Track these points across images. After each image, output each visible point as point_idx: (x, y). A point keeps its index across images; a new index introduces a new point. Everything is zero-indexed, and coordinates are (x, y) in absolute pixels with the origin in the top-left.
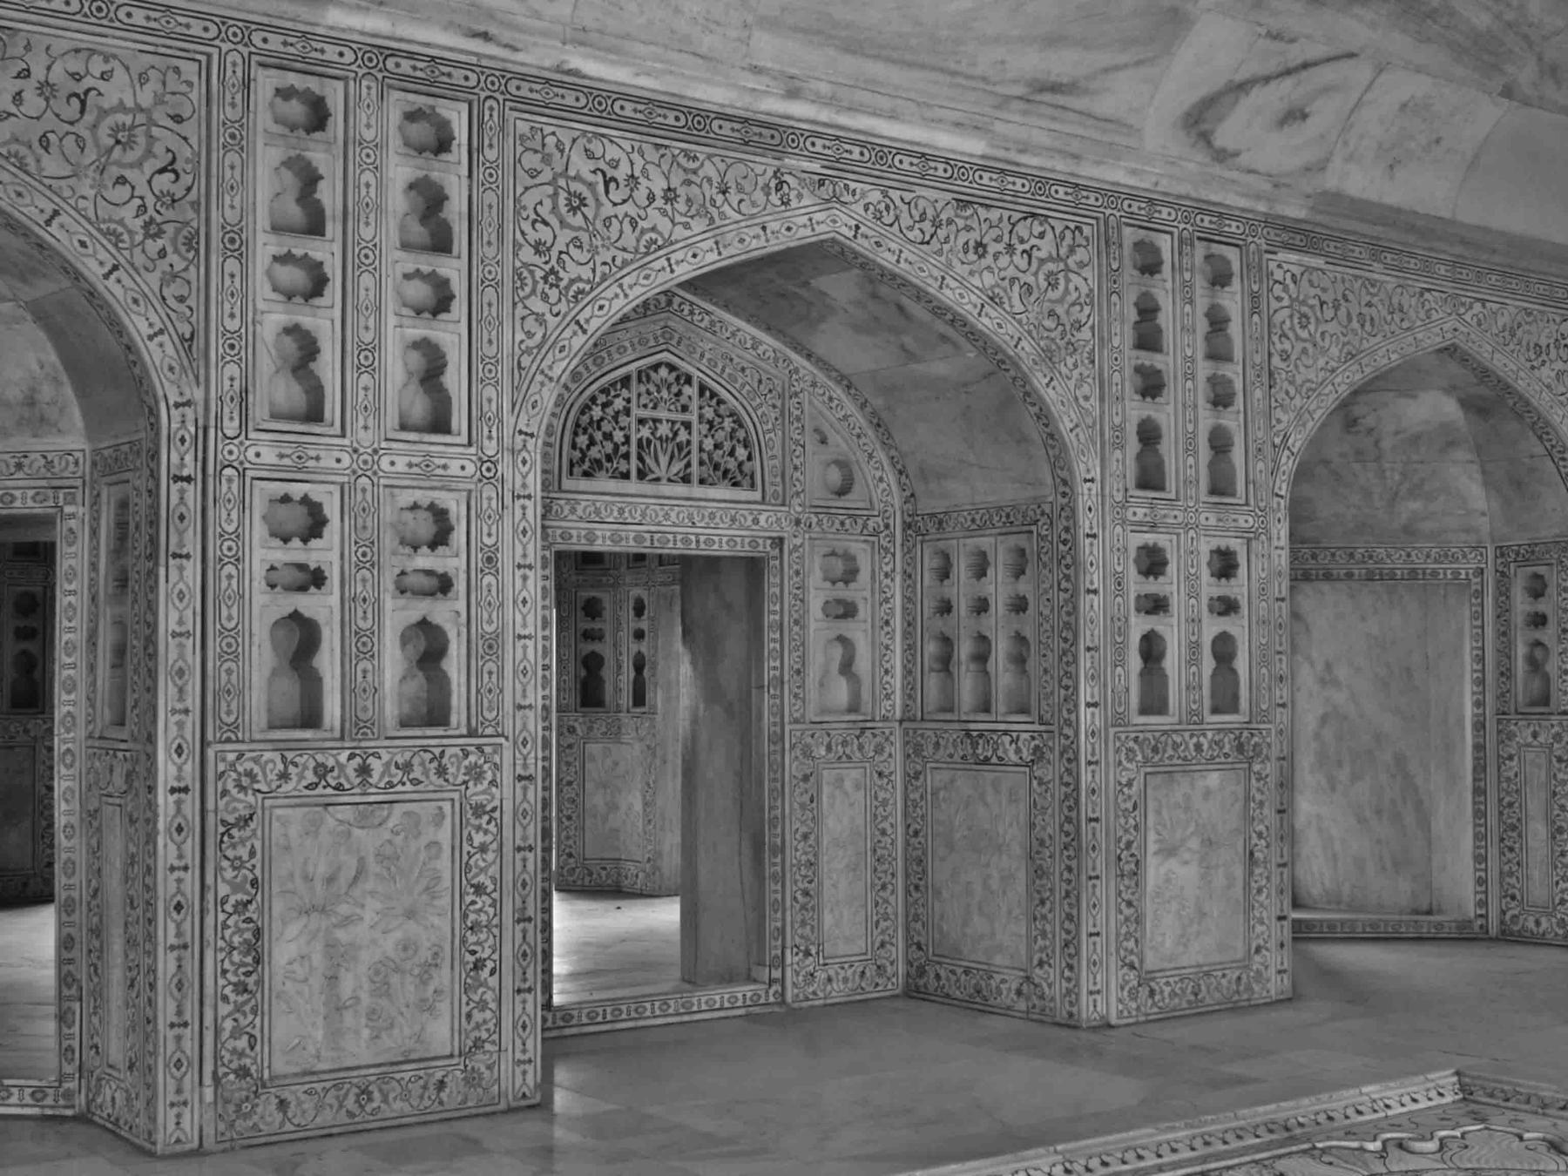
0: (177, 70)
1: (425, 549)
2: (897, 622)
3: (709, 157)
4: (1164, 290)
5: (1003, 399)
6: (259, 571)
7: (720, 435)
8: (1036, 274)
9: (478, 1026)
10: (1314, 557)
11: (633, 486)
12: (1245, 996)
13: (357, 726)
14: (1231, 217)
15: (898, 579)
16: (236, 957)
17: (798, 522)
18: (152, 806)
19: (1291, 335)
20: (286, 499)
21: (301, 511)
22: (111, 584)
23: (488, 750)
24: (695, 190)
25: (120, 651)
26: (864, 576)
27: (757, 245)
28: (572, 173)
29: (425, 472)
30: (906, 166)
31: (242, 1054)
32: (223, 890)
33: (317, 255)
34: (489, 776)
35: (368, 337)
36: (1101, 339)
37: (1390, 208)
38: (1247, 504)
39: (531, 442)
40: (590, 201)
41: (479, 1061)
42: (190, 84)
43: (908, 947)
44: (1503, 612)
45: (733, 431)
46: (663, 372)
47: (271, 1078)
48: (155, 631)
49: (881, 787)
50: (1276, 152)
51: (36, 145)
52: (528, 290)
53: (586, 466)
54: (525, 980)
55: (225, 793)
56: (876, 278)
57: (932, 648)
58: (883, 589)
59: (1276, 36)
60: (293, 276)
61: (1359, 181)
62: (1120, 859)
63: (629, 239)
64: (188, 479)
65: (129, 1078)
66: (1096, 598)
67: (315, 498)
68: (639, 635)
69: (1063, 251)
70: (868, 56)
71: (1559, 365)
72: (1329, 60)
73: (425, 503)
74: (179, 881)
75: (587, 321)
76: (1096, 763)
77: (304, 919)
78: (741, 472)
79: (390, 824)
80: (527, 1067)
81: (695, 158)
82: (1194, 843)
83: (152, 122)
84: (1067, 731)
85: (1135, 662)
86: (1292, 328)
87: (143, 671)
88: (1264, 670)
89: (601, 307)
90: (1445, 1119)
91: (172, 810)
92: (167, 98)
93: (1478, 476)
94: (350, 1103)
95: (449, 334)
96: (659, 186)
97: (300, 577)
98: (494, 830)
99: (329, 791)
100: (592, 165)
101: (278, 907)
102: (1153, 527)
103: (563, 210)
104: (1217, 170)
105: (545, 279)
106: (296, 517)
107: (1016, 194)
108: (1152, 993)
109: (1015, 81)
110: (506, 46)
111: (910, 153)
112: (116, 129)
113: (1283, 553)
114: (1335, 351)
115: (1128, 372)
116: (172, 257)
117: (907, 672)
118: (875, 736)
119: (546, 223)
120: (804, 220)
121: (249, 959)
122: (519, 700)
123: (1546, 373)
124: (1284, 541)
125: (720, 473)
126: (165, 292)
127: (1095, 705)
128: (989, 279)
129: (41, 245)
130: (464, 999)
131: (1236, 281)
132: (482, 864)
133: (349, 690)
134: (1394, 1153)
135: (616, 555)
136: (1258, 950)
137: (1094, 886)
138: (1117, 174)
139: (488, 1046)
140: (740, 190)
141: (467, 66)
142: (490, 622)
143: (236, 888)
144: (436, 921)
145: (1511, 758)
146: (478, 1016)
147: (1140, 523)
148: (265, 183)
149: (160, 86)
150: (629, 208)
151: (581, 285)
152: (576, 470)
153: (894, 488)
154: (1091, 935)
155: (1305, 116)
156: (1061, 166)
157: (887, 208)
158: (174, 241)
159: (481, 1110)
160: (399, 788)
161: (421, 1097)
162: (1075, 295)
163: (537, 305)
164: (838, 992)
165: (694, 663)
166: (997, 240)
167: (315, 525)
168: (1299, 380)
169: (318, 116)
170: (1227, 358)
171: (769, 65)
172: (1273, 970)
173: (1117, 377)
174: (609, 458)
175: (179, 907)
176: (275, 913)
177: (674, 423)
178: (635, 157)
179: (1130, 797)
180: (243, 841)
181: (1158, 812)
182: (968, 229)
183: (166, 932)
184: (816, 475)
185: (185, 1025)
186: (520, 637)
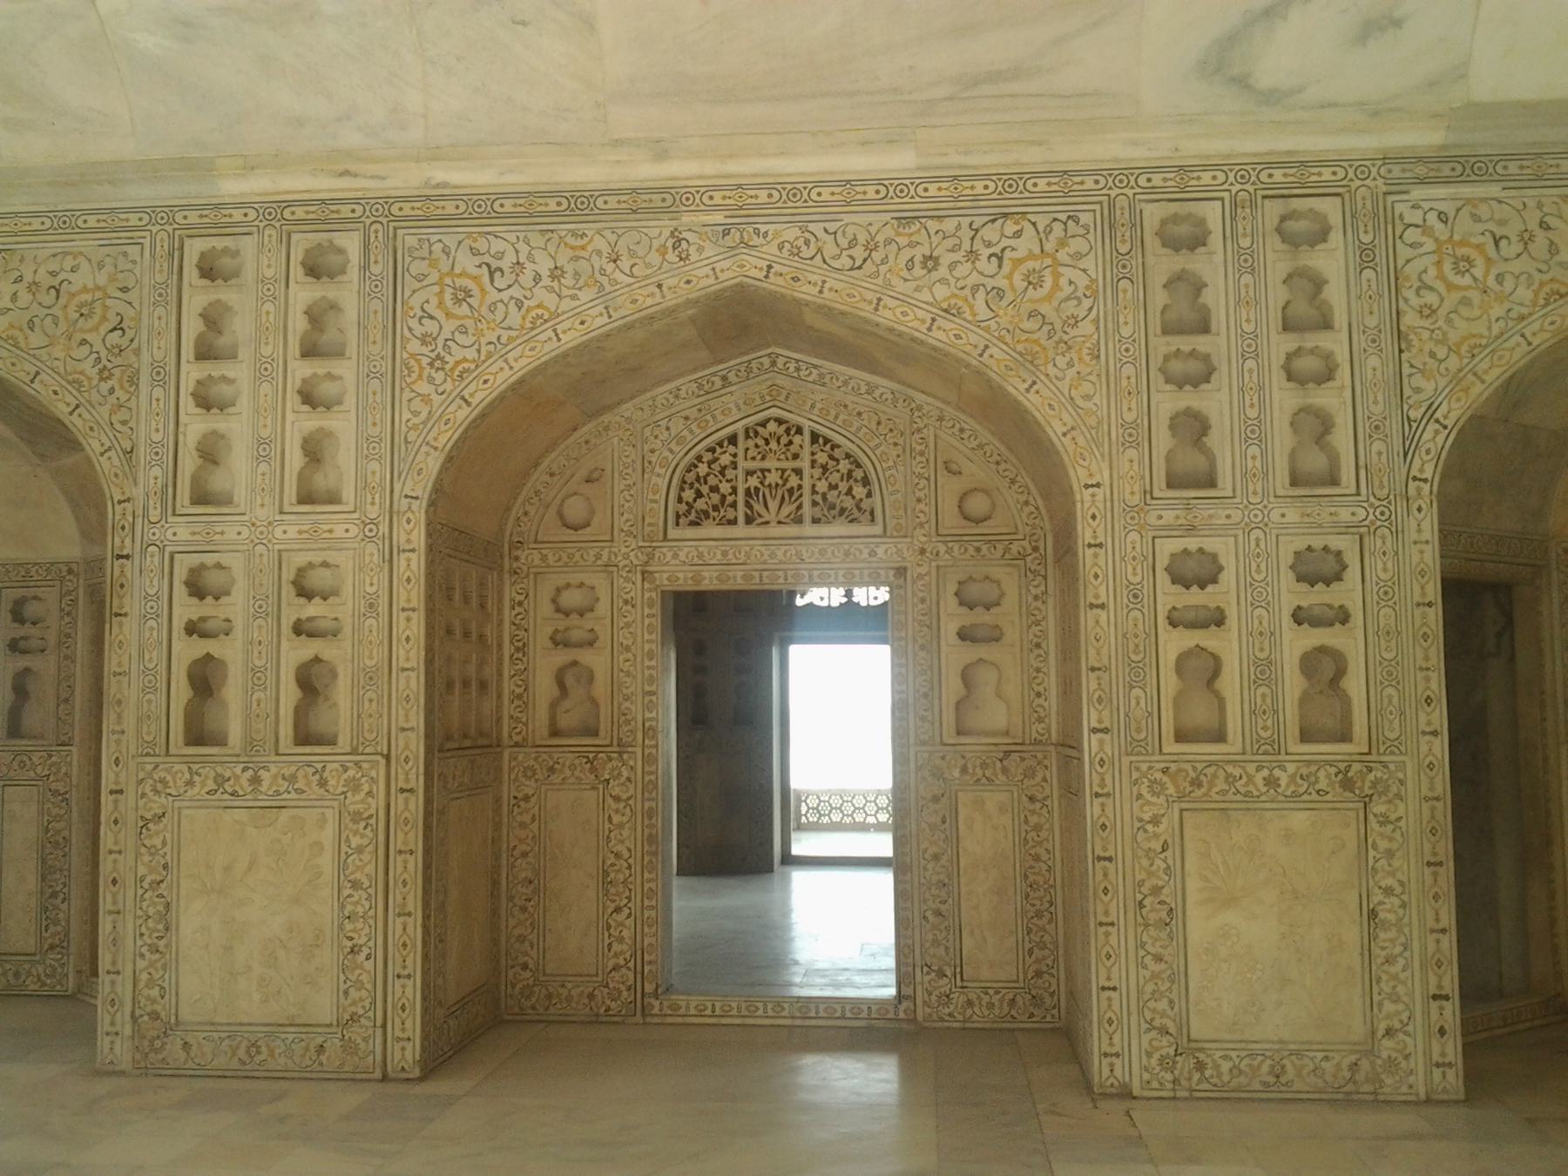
0: (125, 254)
2: (1051, 645)
4: (1210, 265)
8: (1010, 277)
9: (354, 1003)
11: (741, 530)
12: (1367, 1088)
13: (250, 743)
16: (151, 923)
19: (1439, 285)
23: (365, 765)
24: (584, 264)
26: (1011, 601)
28: (457, 271)
31: (154, 1001)
32: (142, 871)
35: (265, 433)
38: (1358, 494)
39: (415, 504)
40: (476, 291)
41: (356, 1033)
42: (134, 262)
45: (850, 474)
46: (772, 426)
47: (177, 1023)
49: (1033, 812)
52: (414, 376)
53: (692, 517)
54: (404, 967)
55: (143, 795)
62: (1141, 905)
63: (515, 318)
64: (127, 557)
66: (1103, 615)
75: (471, 395)
76: (1108, 795)
78: (859, 509)
80: (405, 1043)
86: (1441, 276)
88: (1390, 690)
89: (486, 382)
91: (111, 807)
94: (241, 1053)
96: (544, 266)
98: (371, 835)
99: (226, 796)
102: (1191, 529)
103: (449, 303)
105: (431, 364)
110: (372, 177)
113: (1428, 548)
114: (1525, 294)
116: (119, 393)
118: (1023, 759)
119: (432, 317)
121: (161, 927)
122: (402, 724)
125: (835, 512)
127: (1105, 731)
128: (941, 292)
130: (342, 977)
131: (1336, 237)
132: (358, 863)
136: (1389, 1032)
137: (1107, 934)
140: (632, 253)
141: (357, 201)
146: (353, 993)
150: (516, 292)
151: (466, 365)
153: (1043, 511)
154: (1103, 988)
156: (1032, 158)
157: (807, 243)
158: (120, 380)
159: (359, 1076)
160: (285, 796)
161: (303, 1056)
162: (1068, 290)
163: (424, 388)
166: (952, 251)
168: (1453, 337)
173: (1129, 370)
174: (715, 508)
175: (114, 882)
176: (183, 892)
177: (784, 471)
178: (522, 246)
179: (1156, 836)
180: (157, 833)
182: (912, 245)
186: (404, 670)
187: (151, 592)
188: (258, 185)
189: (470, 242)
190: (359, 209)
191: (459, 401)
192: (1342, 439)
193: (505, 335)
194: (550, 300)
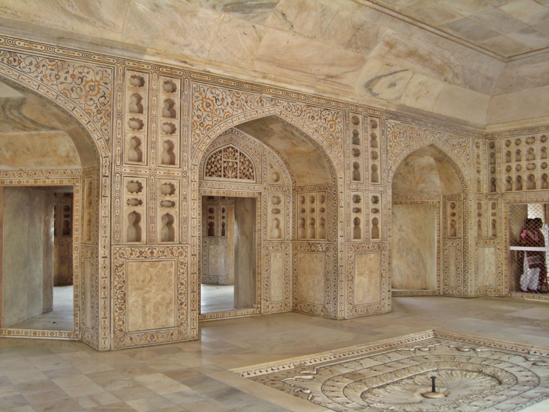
0: (106, 71)
1: (168, 195)
3: (243, 93)
4: (360, 129)
5: (318, 157)
6: (125, 201)
7: (245, 166)
9: (181, 319)
10: (397, 198)
11: (222, 179)
13: (150, 241)
14: (377, 111)
15: (291, 203)
16: (119, 301)
17: (265, 188)
18: (97, 261)
20: (132, 182)
21: (137, 185)
22: (87, 204)
25: (90, 221)
27: (255, 116)
28: (207, 97)
29: (168, 175)
30: (294, 96)
31: (121, 326)
33: (141, 119)
34: (184, 254)
35: (154, 140)
36: (344, 141)
37: (416, 109)
39: (196, 167)
40: (212, 105)
41: (182, 328)
42: (109, 75)
43: (293, 299)
44: (445, 213)
46: (230, 149)
47: (129, 332)
48: (98, 216)
50: (388, 94)
51: (70, 90)
52: (195, 127)
53: (210, 174)
55: (116, 258)
56: (286, 126)
57: (300, 221)
58: (287, 206)
59: (388, 65)
60: (135, 124)
61: (409, 102)
63: (222, 115)
64: (107, 177)
65: (92, 331)
67: (140, 181)
68: (223, 217)
69: (334, 119)
70: (284, 68)
71: (459, 150)
72: (402, 71)
73: (168, 183)
74: (104, 281)
77: (136, 292)
79: (159, 267)
81: (239, 94)
82: (367, 272)
83: (99, 84)
84: (335, 243)
85: (353, 225)
87: (95, 226)
90: (430, 343)
91: (102, 262)
92: (104, 78)
93: (439, 178)
94: (149, 339)
95: (175, 139)
96: (230, 101)
97: (136, 202)
100: (212, 95)
101: (130, 288)
102: (357, 190)
103: (205, 107)
104: (373, 98)
105: (200, 125)
106: (135, 187)
107: (322, 104)
108: (356, 311)
109: (321, 75)
111: (295, 93)
112: (90, 86)
114: (403, 145)
115: (351, 150)
116: (104, 119)
117: (293, 228)
119: (200, 110)
120: (267, 110)
121: (122, 301)
123: (455, 151)
124: (390, 194)
126: (103, 128)
127: (342, 236)
128: (315, 126)
129: (71, 116)
131: (378, 127)
133: (148, 232)
134: (418, 351)
135: (217, 197)
136: (383, 299)
138: (348, 99)
139: (184, 325)
140: (251, 102)
142: (185, 214)
143: (119, 283)
144: (171, 292)
145: (446, 250)
146: (181, 317)
147: (354, 189)
148: (128, 100)
149: (101, 76)
150: (222, 107)
152: (208, 174)
153: (290, 180)
155: (395, 85)
156: (334, 97)
158: (104, 115)
163: (198, 131)
164: (275, 310)
165: (238, 225)
166: (317, 115)
167: (140, 189)
168: (394, 152)
169: (142, 83)
170: (376, 147)
171: (258, 70)
172: (387, 304)
173: (348, 151)
174: (216, 172)
175: (104, 288)
176: (129, 289)
178: (224, 93)
180: (121, 271)
181: (358, 264)
182: (310, 113)
183: (101, 294)
184: (270, 176)
185: (106, 318)
187: (118, 189)
188: (157, 59)
189: (210, 89)
190: (182, 73)
191: (207, 137)
192: (379, 172)
193: (220, 119)
194: (231, 111)
